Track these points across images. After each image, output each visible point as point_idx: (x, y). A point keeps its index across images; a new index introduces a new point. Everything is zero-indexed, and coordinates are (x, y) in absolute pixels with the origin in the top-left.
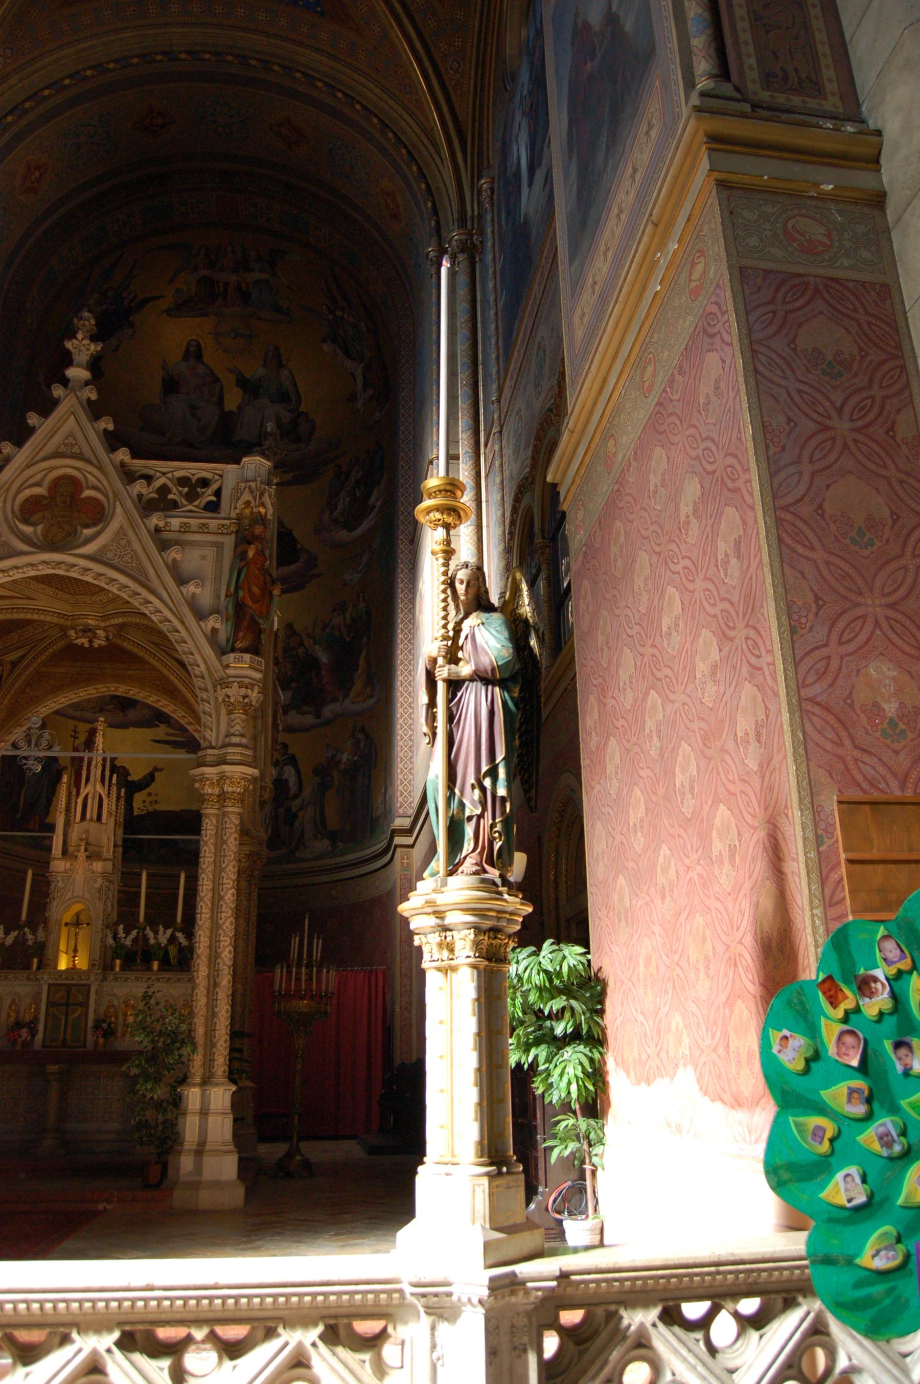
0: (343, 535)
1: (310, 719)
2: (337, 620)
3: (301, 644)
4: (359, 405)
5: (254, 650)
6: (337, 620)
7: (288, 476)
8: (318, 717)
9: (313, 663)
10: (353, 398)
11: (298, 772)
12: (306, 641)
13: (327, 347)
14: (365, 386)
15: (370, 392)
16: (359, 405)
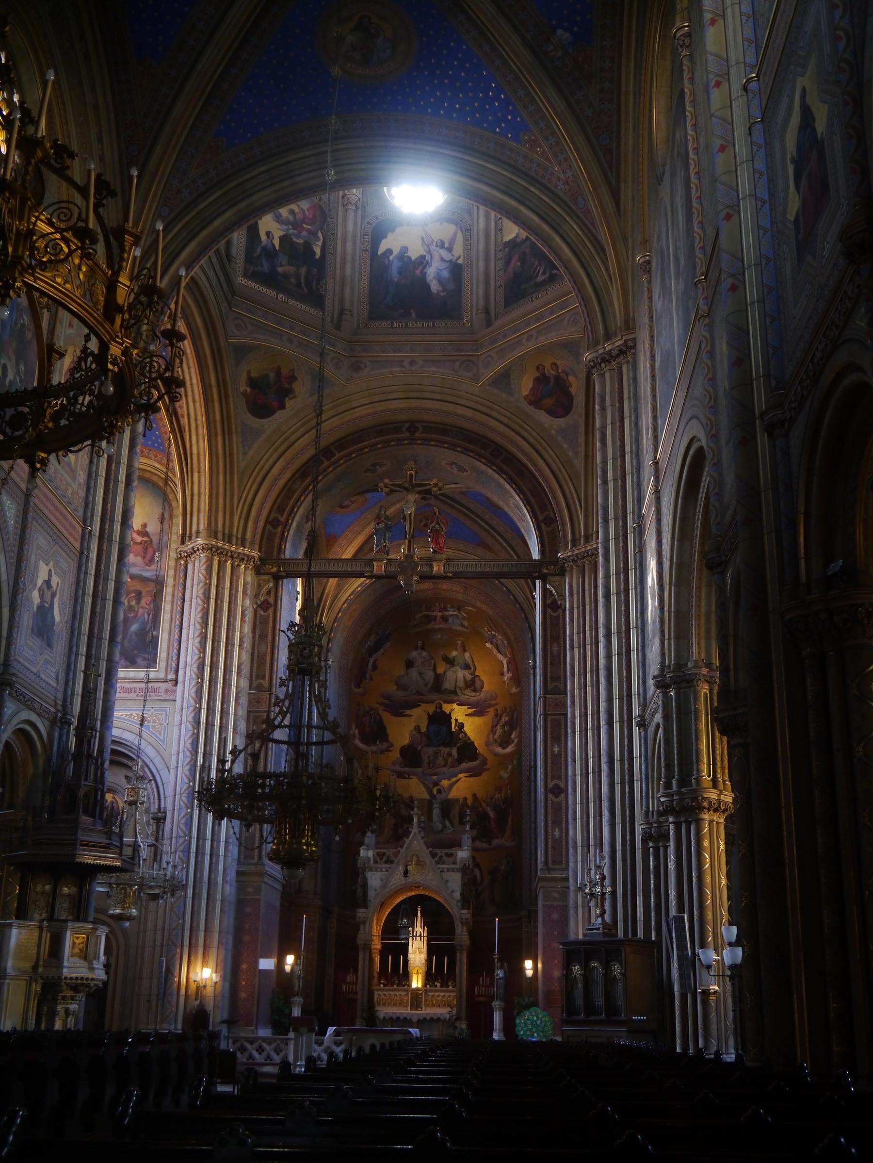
0: (499, 750)
1: (485, 845)
2: (497, 796)
3: (481, 805)
4: (506, 678)
5: (468, 908)
6: (497, 796)
7: (471, 711)
8: (490, 844)
9: (485, 816)
10: (502, 674)
11: (481, 871)
12: (484, 805)
13: (488, 645)
14: (508, 670)
15: (510, 675)
16: (506, 678)
